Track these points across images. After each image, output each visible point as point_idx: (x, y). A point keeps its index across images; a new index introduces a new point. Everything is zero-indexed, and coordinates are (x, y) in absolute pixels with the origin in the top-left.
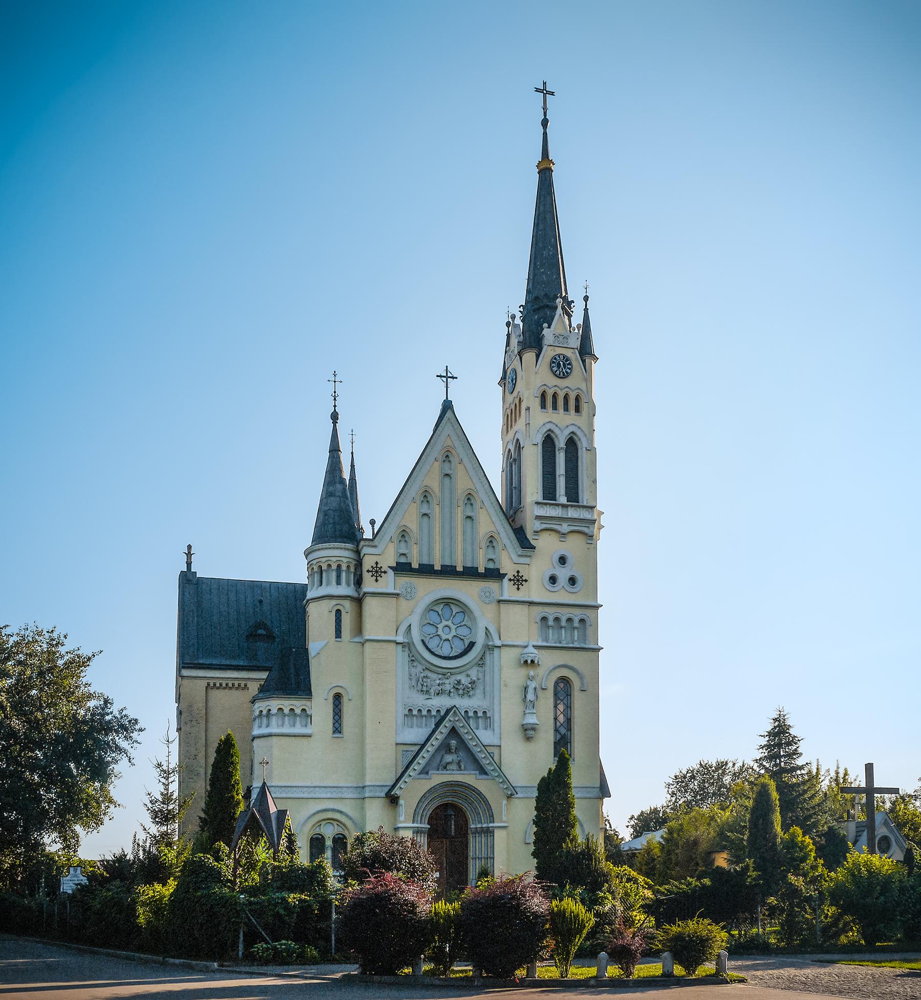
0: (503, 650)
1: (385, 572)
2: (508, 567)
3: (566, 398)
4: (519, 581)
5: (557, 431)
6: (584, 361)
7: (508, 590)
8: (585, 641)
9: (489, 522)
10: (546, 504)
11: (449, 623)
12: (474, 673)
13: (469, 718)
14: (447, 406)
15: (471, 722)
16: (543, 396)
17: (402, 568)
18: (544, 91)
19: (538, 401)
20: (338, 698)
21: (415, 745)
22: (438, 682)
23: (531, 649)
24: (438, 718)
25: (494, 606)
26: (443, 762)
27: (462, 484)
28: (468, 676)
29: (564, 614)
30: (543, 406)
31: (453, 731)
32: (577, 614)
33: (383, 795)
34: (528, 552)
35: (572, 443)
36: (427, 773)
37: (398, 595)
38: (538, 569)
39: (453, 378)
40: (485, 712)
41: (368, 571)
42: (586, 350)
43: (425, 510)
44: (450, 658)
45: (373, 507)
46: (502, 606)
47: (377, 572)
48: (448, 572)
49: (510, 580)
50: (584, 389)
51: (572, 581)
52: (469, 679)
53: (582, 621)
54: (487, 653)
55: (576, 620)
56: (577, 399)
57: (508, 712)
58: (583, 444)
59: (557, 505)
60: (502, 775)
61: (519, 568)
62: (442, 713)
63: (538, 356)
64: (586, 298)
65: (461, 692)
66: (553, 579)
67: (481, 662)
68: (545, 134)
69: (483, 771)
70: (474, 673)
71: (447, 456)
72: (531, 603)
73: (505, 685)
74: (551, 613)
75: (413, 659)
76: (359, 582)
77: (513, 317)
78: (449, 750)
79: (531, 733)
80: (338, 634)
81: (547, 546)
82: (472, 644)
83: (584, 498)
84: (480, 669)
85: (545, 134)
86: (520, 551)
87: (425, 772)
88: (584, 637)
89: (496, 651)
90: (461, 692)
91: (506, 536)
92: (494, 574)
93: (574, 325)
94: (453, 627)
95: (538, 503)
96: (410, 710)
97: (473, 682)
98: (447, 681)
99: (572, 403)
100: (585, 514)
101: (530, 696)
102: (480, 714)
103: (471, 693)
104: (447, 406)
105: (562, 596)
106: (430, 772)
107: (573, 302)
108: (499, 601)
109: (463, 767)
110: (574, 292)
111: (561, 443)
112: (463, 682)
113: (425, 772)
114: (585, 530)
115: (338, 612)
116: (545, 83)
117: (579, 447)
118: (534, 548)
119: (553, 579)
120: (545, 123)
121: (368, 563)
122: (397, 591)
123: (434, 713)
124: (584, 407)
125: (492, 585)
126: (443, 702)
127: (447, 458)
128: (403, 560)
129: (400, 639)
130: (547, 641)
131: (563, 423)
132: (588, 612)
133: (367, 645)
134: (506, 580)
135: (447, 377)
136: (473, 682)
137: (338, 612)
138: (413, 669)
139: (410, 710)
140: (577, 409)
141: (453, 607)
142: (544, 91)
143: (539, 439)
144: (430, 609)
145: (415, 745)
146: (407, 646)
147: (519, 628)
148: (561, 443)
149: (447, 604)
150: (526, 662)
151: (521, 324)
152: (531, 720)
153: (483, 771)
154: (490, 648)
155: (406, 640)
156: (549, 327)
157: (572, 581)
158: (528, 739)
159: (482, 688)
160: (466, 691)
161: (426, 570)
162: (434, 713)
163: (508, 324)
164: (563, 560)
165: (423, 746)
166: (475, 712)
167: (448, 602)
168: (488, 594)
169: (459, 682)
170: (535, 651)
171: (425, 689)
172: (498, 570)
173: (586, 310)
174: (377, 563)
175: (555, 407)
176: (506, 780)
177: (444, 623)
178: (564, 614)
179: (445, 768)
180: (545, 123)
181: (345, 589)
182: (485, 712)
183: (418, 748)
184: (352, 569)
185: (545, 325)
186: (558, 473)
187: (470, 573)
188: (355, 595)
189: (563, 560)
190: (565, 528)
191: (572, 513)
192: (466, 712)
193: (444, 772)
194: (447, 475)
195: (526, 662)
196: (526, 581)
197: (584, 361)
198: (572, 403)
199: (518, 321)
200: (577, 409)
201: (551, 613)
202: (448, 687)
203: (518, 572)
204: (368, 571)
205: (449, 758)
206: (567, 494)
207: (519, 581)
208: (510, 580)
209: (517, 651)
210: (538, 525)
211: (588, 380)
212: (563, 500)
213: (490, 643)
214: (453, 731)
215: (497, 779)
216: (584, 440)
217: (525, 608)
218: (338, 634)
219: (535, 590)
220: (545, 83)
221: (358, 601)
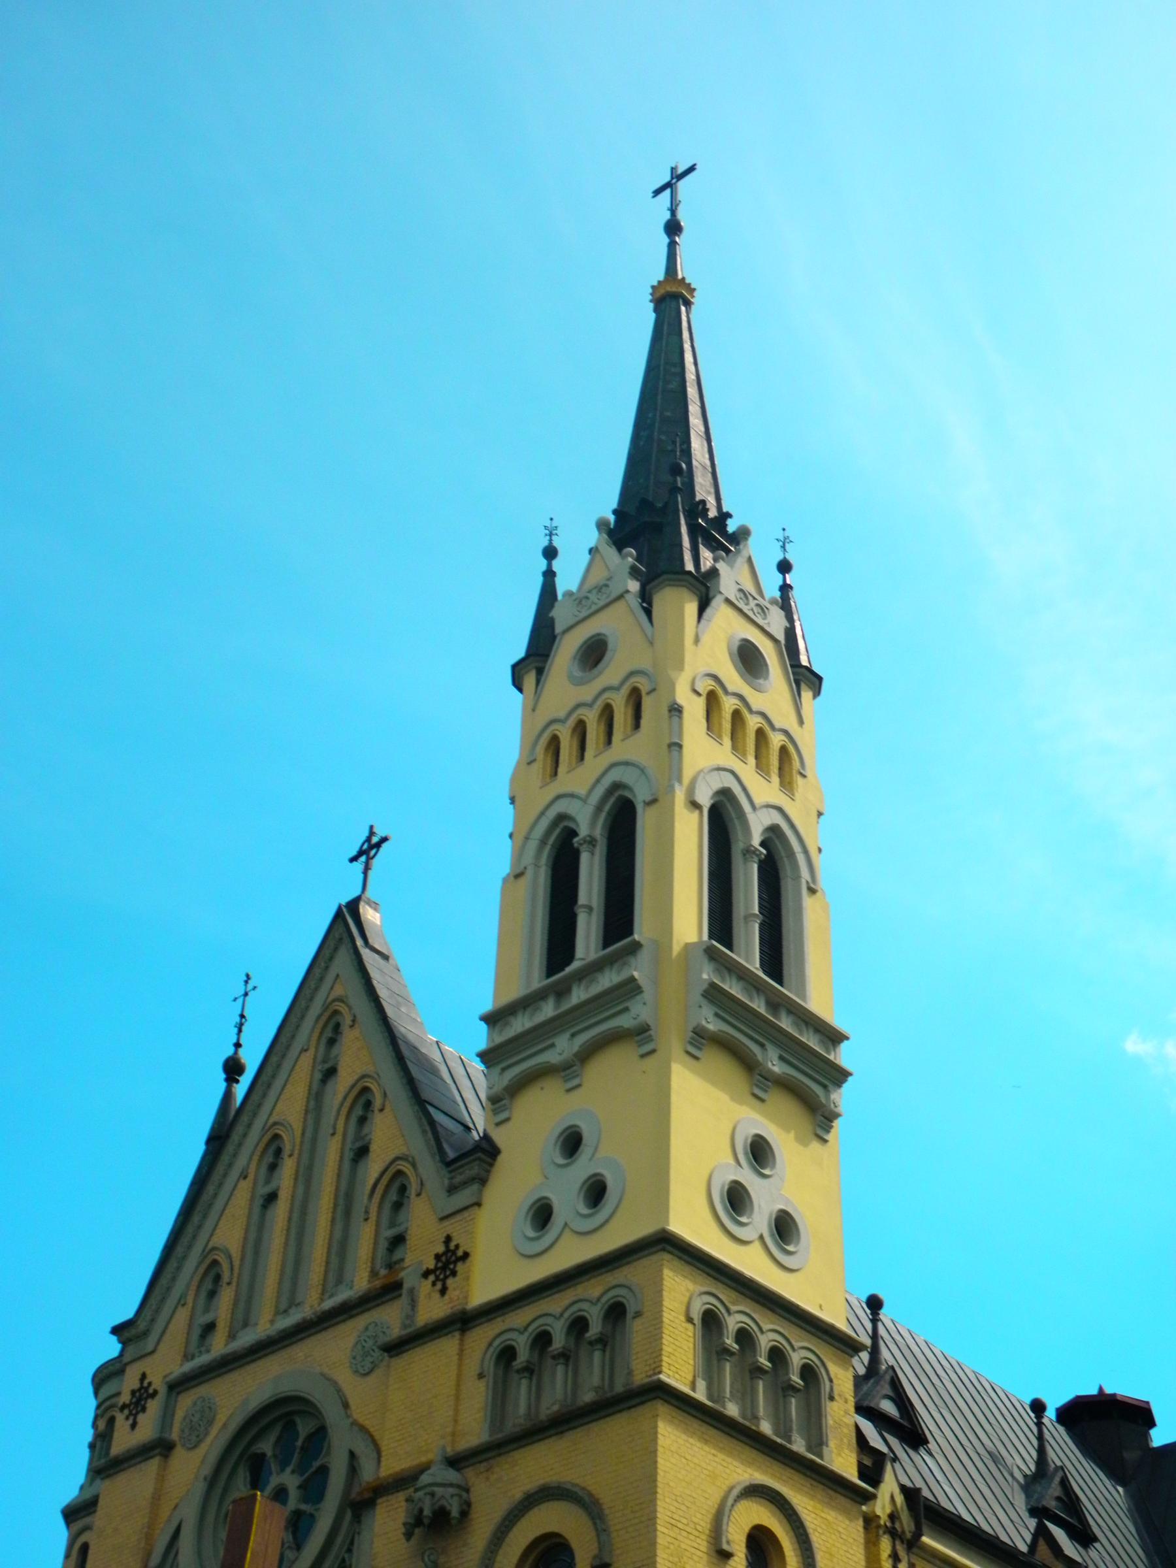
29: (554, 1312)
32: (591, 1296)
51: (596, 1192)
56: (636, 700)
58: (640, 795)
66: (542, 1214)
85: (672, 246)
99: (621, 717)
105: (569, 1253)
114: (625, 1022)
119: (542, 1214)
120: (673, 228)
124: (647, 703)
135: (370, 848)
157: (596, 1192)
164: (572, 1143)
170: (452, 1475)
178: (554, 1312)
180: (673, 228)
189: (572, 1143)
190: (564, 1047)
198: (621, 717)
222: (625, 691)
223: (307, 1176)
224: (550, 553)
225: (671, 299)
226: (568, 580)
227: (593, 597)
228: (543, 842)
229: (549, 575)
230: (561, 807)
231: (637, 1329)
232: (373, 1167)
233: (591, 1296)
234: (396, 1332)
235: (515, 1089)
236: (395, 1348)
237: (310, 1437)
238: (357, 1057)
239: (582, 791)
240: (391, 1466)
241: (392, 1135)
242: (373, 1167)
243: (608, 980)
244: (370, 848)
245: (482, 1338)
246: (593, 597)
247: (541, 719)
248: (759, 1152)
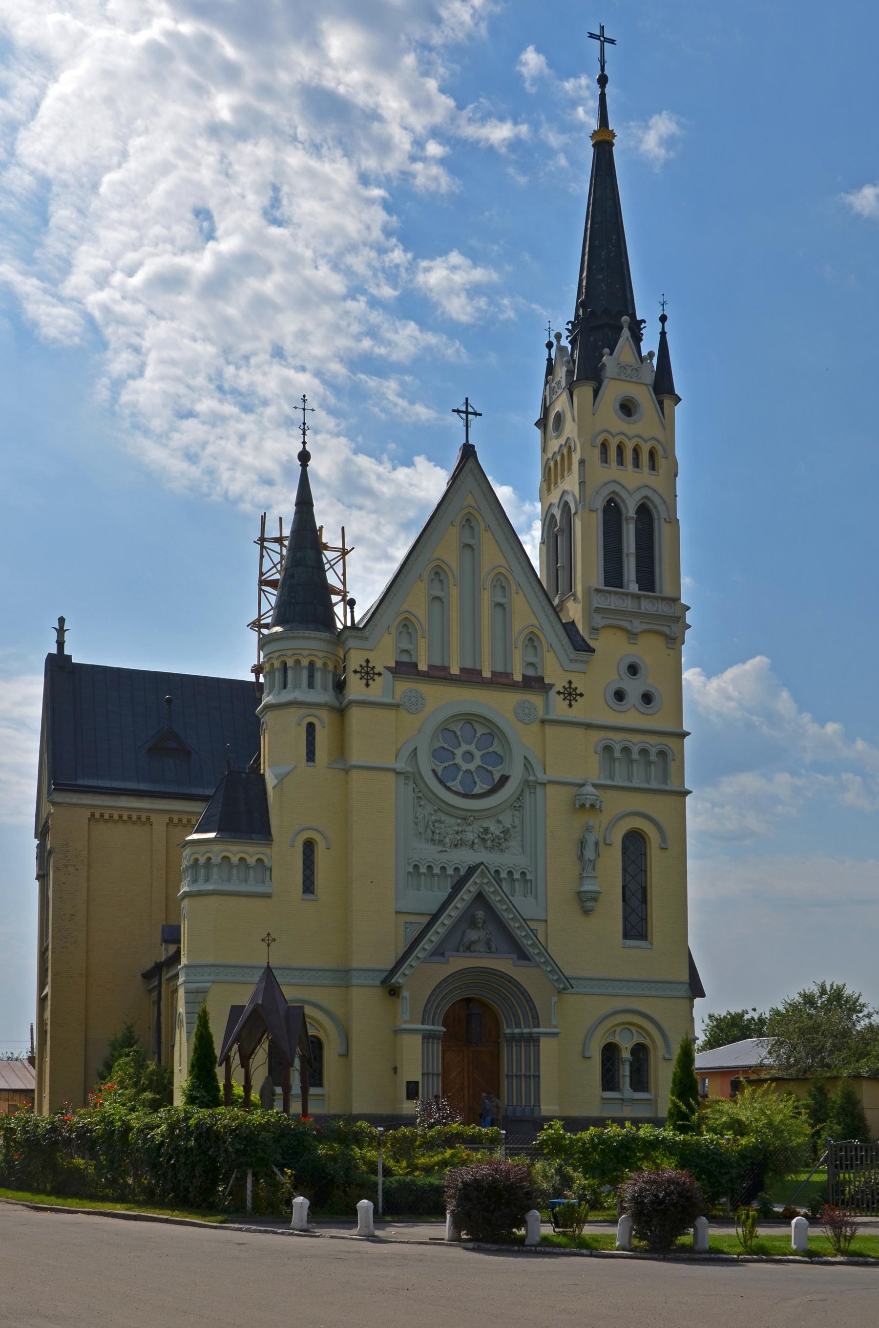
0: (549, 788)
1: (379, 674)
2: (555, 674)
3: (636, 451)
4: (571, 694)
6: (661, 403)
8: (665, 783)
9: (525, 613)
10: (609, 592)
11: (472, 748)
12: (507, 819)
13: (501, 880)
14: (468, 452)
15: (504, 885)
16: (604, 446)
17: (405, 669)
18: (602, 38)
19: (597, 451)
20: (309, 847)
21: (424, 914)
22: (456, 828)
23: (589, 789)
24: (456, 879)
25: (535, 728)
26: (466, 940)
27: (491, 556)
28: (499, 822)
30: (605, 459)
31: (480, 898)
33: (378, 983)
34: (583, 656)
35: (645, 512)
36: (442, 955)
37: (396, 706)
38: (599, 676)
39: (476, 414)
40: (523, 874)
41: (355, 672)
42: (663, 385)
43: (437, 593)
44: (470, 770)
45: (362, 582)
46: (547, 727)
47: (367, 673)
48: (470, 677)
49: (559, 693)
50: (660, 435)
51: (647, 698)
52: (501, 826)
53: (662, 754)
54: (527, 791)
55: (653, 751)
57: (558, 874)
58: (660, 511)
59: (627, 594)
60: (550, 960)
62: (462, 873)
63: (596, 392)
64: (663, 319)
65: (489, 843)
66: (620, 695)
68: (603, 97)
69: (523, 956)
70: (507, 819)
71: (468, 520)
72: (589, 726)
75: (422, 794)
76: (340, 686)
77: (558, 336)
78: (473, 924)
79: (590, 904)
80: (311, 756)
81: (611, 648)
82: (504, 779)
83: (665, 589)
84: (516, 813)
85: (603, 97)
86: (573, 654)
87: (439, 952)
88: (665, 776)
89: (539, 789)
90: (489, 843)
91: (552, 638)
92: (534, 683)
93: (644, 353)
94: (478, 754)
95: (598, 591)
96: (416, 867)
97: (506, 832)
98: (470, 828)
99: (645, 458)
100: (663, 608)
101: (589, 854)
102: (517, 876)
103: (504, 845)
104: (468, 452)
106: (447, 954)
107: (644, 321)
108: (543, 722)
109: (493, 949)
110: (645, 308)
111: (630, 510)
112: (492, 829)
113: (439, 952)
115: (311, 727)
116: (602, 28)
117: (655, 516)
118: (593, 651)
119: (620, 695)
121: (355, 660)
122: (397, 700)
123: (450, 872)
124: (661, 462)
125: (536, 700)
126: (465, 857)
127: (468, 522)
128: (405, 658)
129: (400, 766)
130: (612, 778)
131: (632, 483)
133: (355, 774)
134: (552, 693)
136: (506, 832)
137: (311, 727)
138: (420, 809)
139: (416, 867)
140: (653, 467)
141: (476, 725)
142: (602, 38)
143: (600, 504)
144: (444, 729)
145: (424, 914)
146: (410, 777)
147: (573, 759)
148: (630, 510)
149: (469, 722)
150: (583, 806)
151: (569, 347)
153: (523, 956)
154: (530, 785)
155: (410, 769)
156: (611, 354)
157: (647, 698)
159: (519, 838)
160: (498, 844)
161: (439, 674)
162: (450, 872)
163: (549, 345)
164: (633, 670)
165: (435, 917)
166: (510, 873)
167: (470, 719)
168: (527, 711)
169: (486, 830)
171: (437, 837)
172: (543, 678)
173: (663, 334)
174: (368, 661)
175: (621, 462)
176: (556, 969)
177: (465, 747)
179: (468, 948)
181: (323, 695)
182: (523, 874)
183: (425, 920)
184: (331, 667)
185: (606, 350)
186: (625, 551)
187: (501, 681)
188: (337, 704)
189: (633, 670)
190: (637, 625)
191: (646, 606)
192: (497, 872)
193: (468, 954)
194: (469, 546)
195: (583, 806)
196: (581, 695)
197: (661, 403)
198: (645, 458)
199: (565, 342)
202: (470, 836)
203: (570, 682)
204: (355, 672)
205: (473, 935)
206: (638, 581)
207: (571, 694)
208: (559, 693)
210: (599, 621)
211: (668, 426)
212: (634, 588)
213: (532, 778)
214: (480, 898)
215: (544, 967)
216: (662, 508)
217: (580, 732)
218: (311, 756)
219: (594, 707)
220: (602, 28)
221: (341, 712)
227: (629, 371)
239: (631, 487)
246: (629, 371)
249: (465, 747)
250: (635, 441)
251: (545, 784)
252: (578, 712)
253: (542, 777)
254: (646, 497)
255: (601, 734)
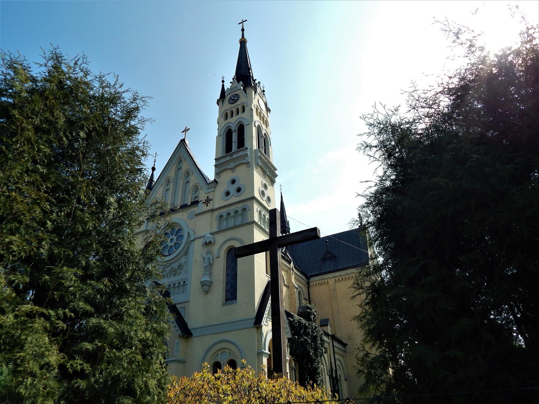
5: (231, 125)
6: (246, 92)
7: (202, 207)
17: (152, 217)
29: (232, 209)
32: (239, 207)
40: (185, 282)
49: (203, 203)
50: (245, 101)
58: (245, 123)
61: (207, 195)
67: (186, 253)
72: (212, 211)
73: (195, 262)
74: (224, 211)
92: (195, 203)
98: (168, 269)
114: (245, 161)
119: (228, 194)
120: (243, 30)
124: (246, 108)
132: (248, 203)
134: (200, 204)
135: (186, 130)
148: (234, 128)
152: (207, 278)
157: (239, 190)
158: (207, 292)
170: (211, 236)
178: (232, 209)
180: (243, 30)
187: (184, 207)
189: (233, 182)
190: (232, 165)
197: (246, 92)
198: (241, 110)
200: (244, 111)
201: (224, 211)
208: (203, 203)
209: (202, 239)
222: (241, 105)
223: (175, 186)
224: (223, 81)
225: (243, 43)
226: (228, 86)
228: (225, 130)
229: (223, 85)
230: (229, 125)
231: (249, 213)
232: (191, 185)
233: (239, 207)
234: (197, 213)
235: (221, 172)
236: (197, 215)
237: (178, 230)
238: (185, 166)
240: (197, 235)
241: (194, 179)
242: (191, 185)
243: (241, 154)
244: (186, 130)
245: (216, 214)
247: (223, 110)
248: (265, 186)
249: (171, 237)
250: (236, 108)
251: (193, 240)
252: (210, 207)
253: (192, 238)
254: (240, 122)
255: (219, 212)
